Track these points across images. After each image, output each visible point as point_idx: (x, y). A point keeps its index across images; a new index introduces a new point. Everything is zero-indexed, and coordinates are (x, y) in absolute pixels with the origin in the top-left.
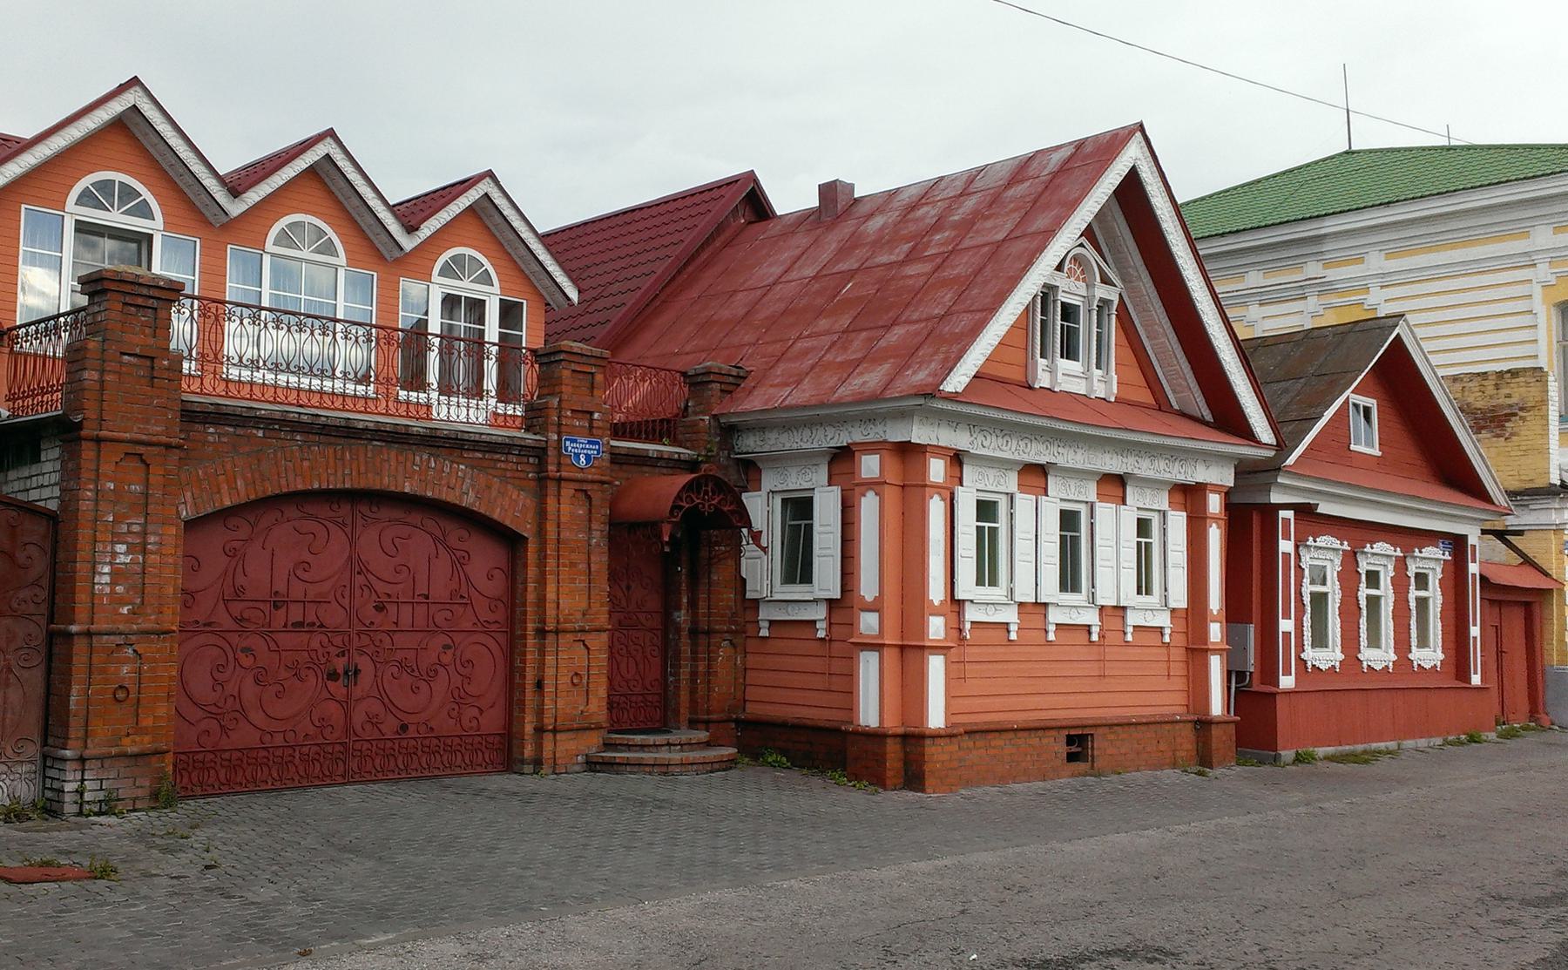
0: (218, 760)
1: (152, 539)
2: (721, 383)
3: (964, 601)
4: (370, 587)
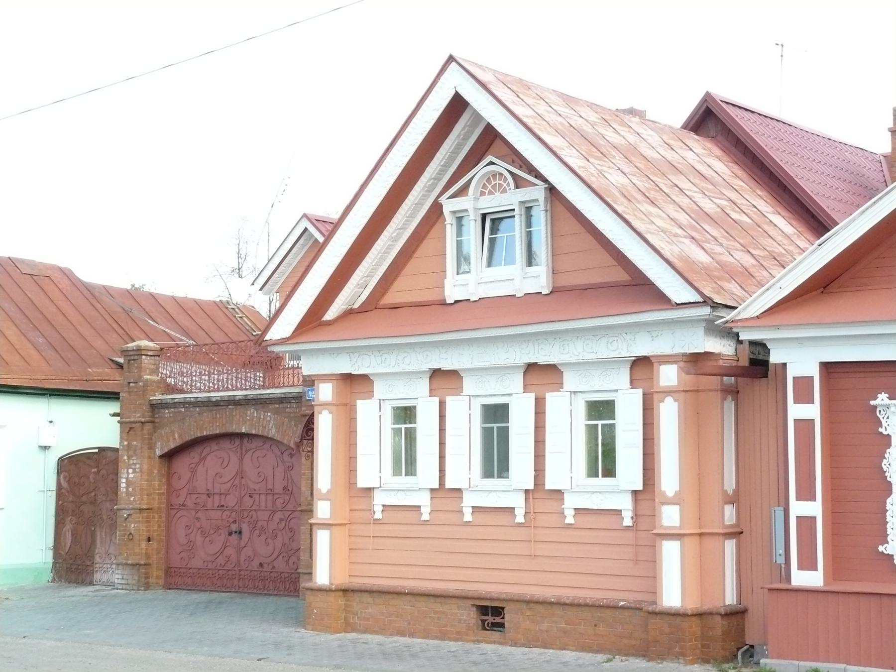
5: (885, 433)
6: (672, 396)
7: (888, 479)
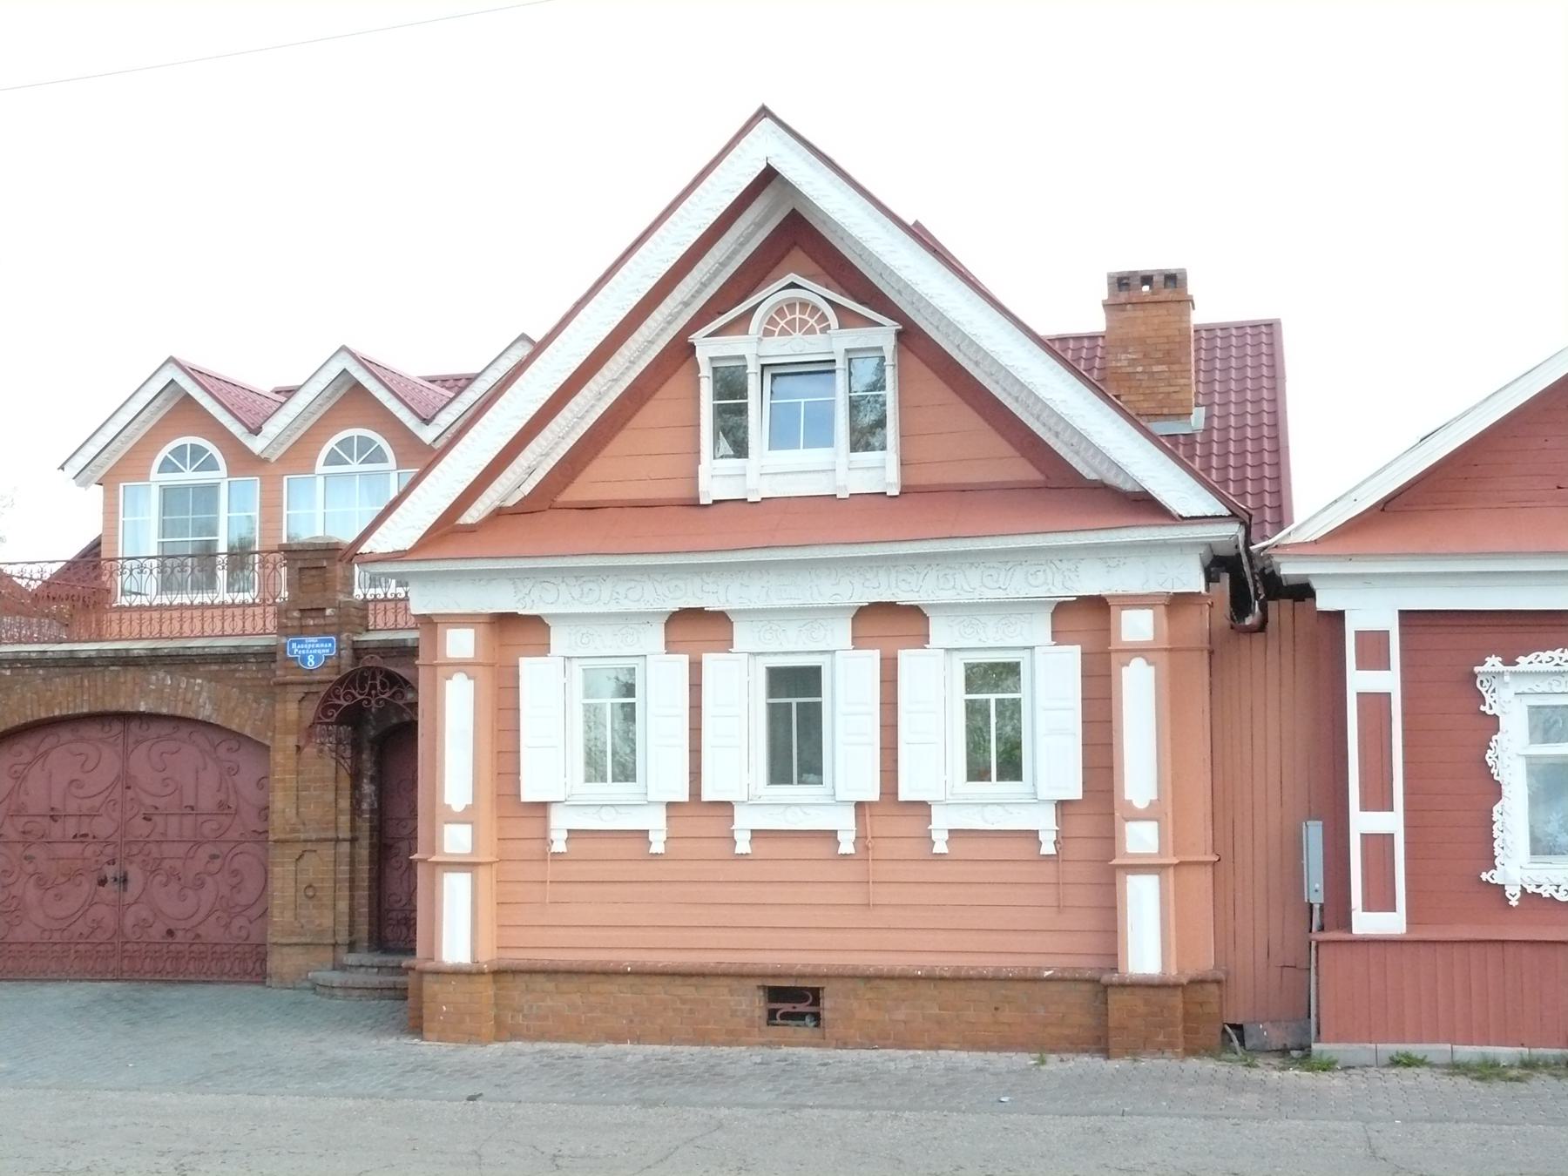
5: (1489, 712)
6: (1143, 657)
7: (1496, 778)
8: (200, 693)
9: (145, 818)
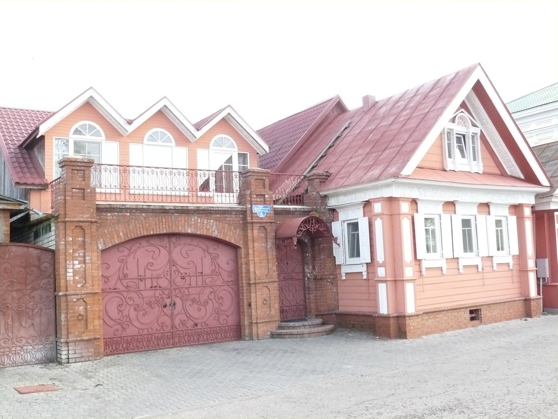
0: (122, 340)
1: (87, 258)
2: (320, 179)
3: (422, 260)
4: (178, 271)
8: (212, 226)
9: (181, 278)
